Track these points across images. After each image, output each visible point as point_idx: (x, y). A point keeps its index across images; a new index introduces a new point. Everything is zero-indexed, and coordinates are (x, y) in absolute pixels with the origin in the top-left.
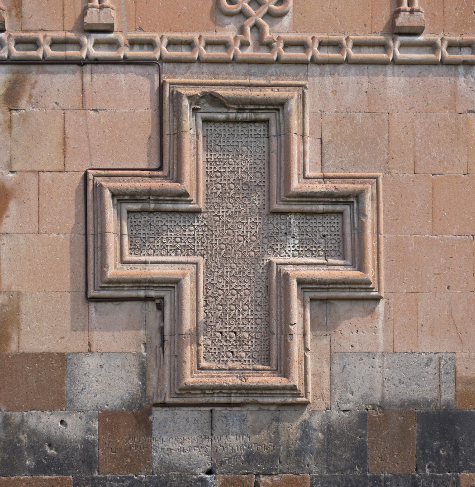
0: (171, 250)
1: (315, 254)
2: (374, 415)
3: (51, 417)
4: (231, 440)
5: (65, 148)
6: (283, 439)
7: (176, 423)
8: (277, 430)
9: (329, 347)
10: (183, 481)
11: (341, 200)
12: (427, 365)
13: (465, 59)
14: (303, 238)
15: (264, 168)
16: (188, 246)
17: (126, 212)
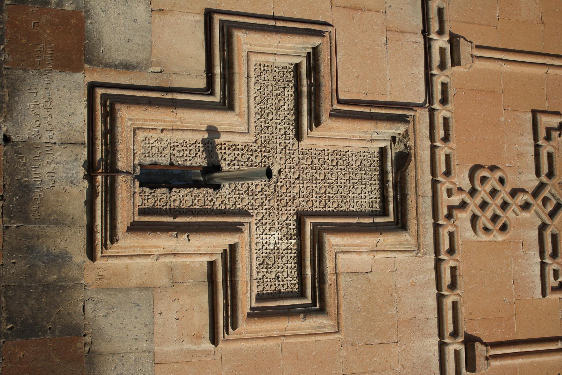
2: (79, 344)
4: (48, 166)
5: (352, 9)
6: (49, 231)
8: (60, 223)
9: (159, 285)
14: (276, 253)
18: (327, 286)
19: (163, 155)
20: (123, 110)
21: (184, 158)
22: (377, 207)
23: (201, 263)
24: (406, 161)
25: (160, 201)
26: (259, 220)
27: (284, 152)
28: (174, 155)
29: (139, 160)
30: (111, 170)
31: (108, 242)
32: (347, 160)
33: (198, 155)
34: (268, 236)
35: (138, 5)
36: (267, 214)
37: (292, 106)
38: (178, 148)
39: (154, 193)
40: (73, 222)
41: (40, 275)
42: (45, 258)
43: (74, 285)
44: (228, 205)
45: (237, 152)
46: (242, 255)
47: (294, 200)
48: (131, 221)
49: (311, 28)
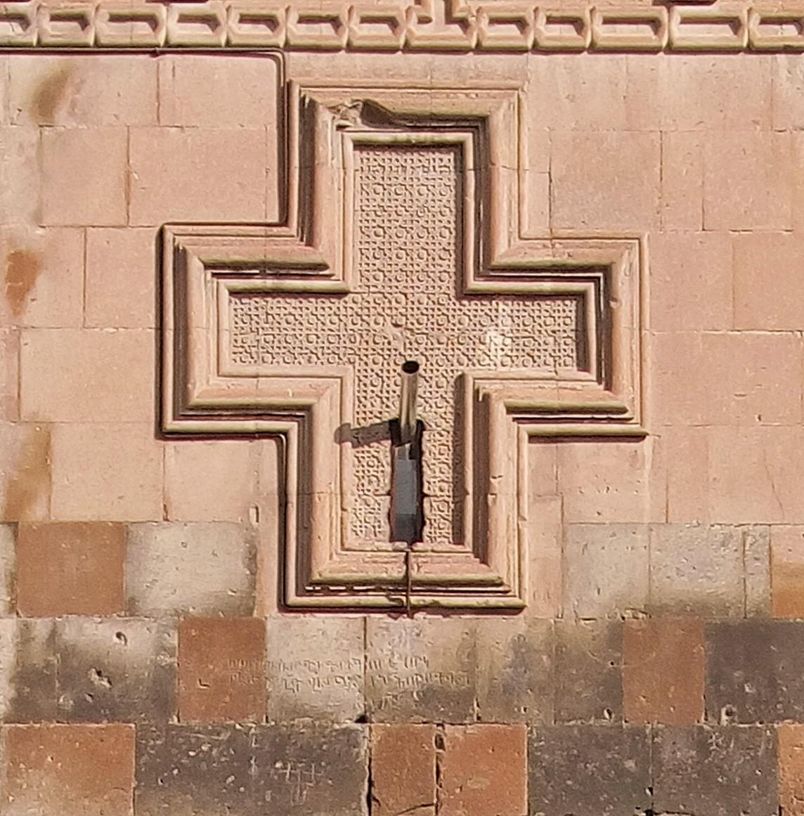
4: (397, 666)
7: (305, 638)
10: (317, 734)
17: (227, 292)
19: (377, 506)
20: (320, 569)
22: (449, 158)
23: (530, 451)
25: (443, 511)
26: (470, 360)
27: (365, 318)
28: (377, 490)
29: (384, 541)
30: (405, 584)
31: (501, 589)
32: (377, 208)
33: (376, 454)
34: (493, 347)
35: (162, 540)
36: (460, 347)
37: (294, 302)
38: (366, 484)
39: (430, 520)
40: (472, 633)
41: (542, 677)
42: (519, 670)
44: (448, 409)
47: (439, 304)
48: (472, 556)
49: (171, 267)
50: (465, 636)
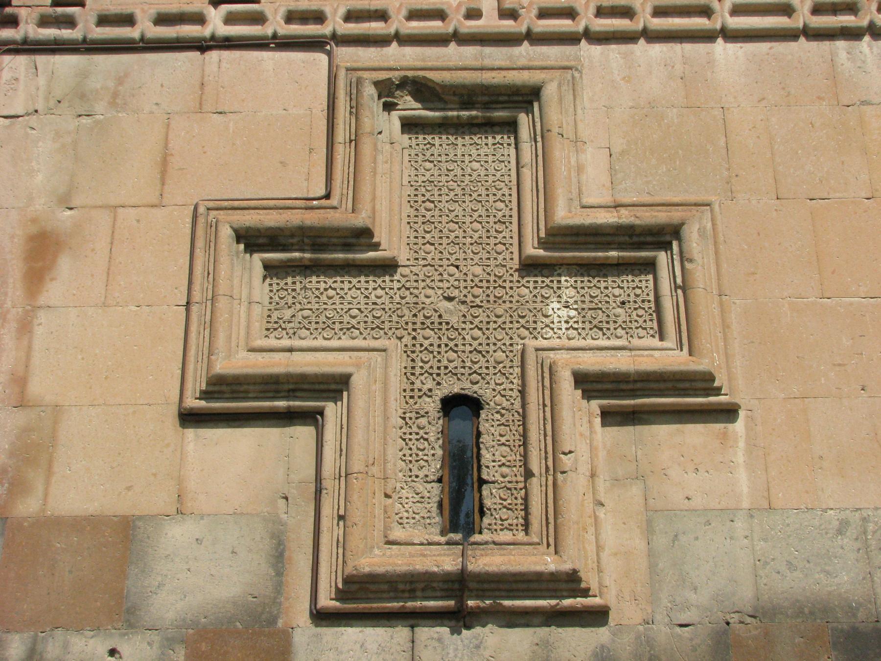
0: (341, 329)
1: (608, 333)
3: (92, 641)
7: (341, 653)
9: (642, 501)
11: (649, 239)
12: (840, 532)
13: (844, 25)
15: (510, 195)
16: (373, 322)
18: (638, 222)
21: (430, 458)
24: (426, 86)
28: (427, 476)
29: (436, 535)
33: (426, 436)
36: (520, 320)
43: (648, 642)
45: (418, 371)
46: (592, 362)
50: (536, 648)
